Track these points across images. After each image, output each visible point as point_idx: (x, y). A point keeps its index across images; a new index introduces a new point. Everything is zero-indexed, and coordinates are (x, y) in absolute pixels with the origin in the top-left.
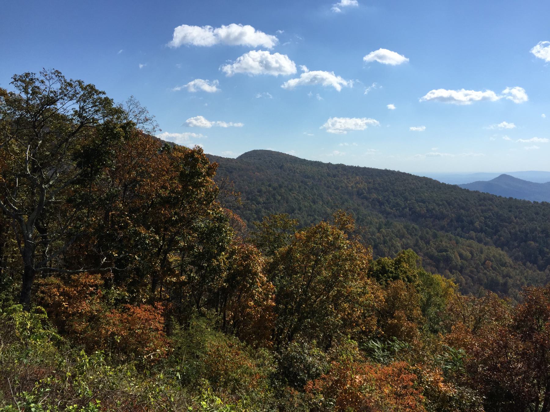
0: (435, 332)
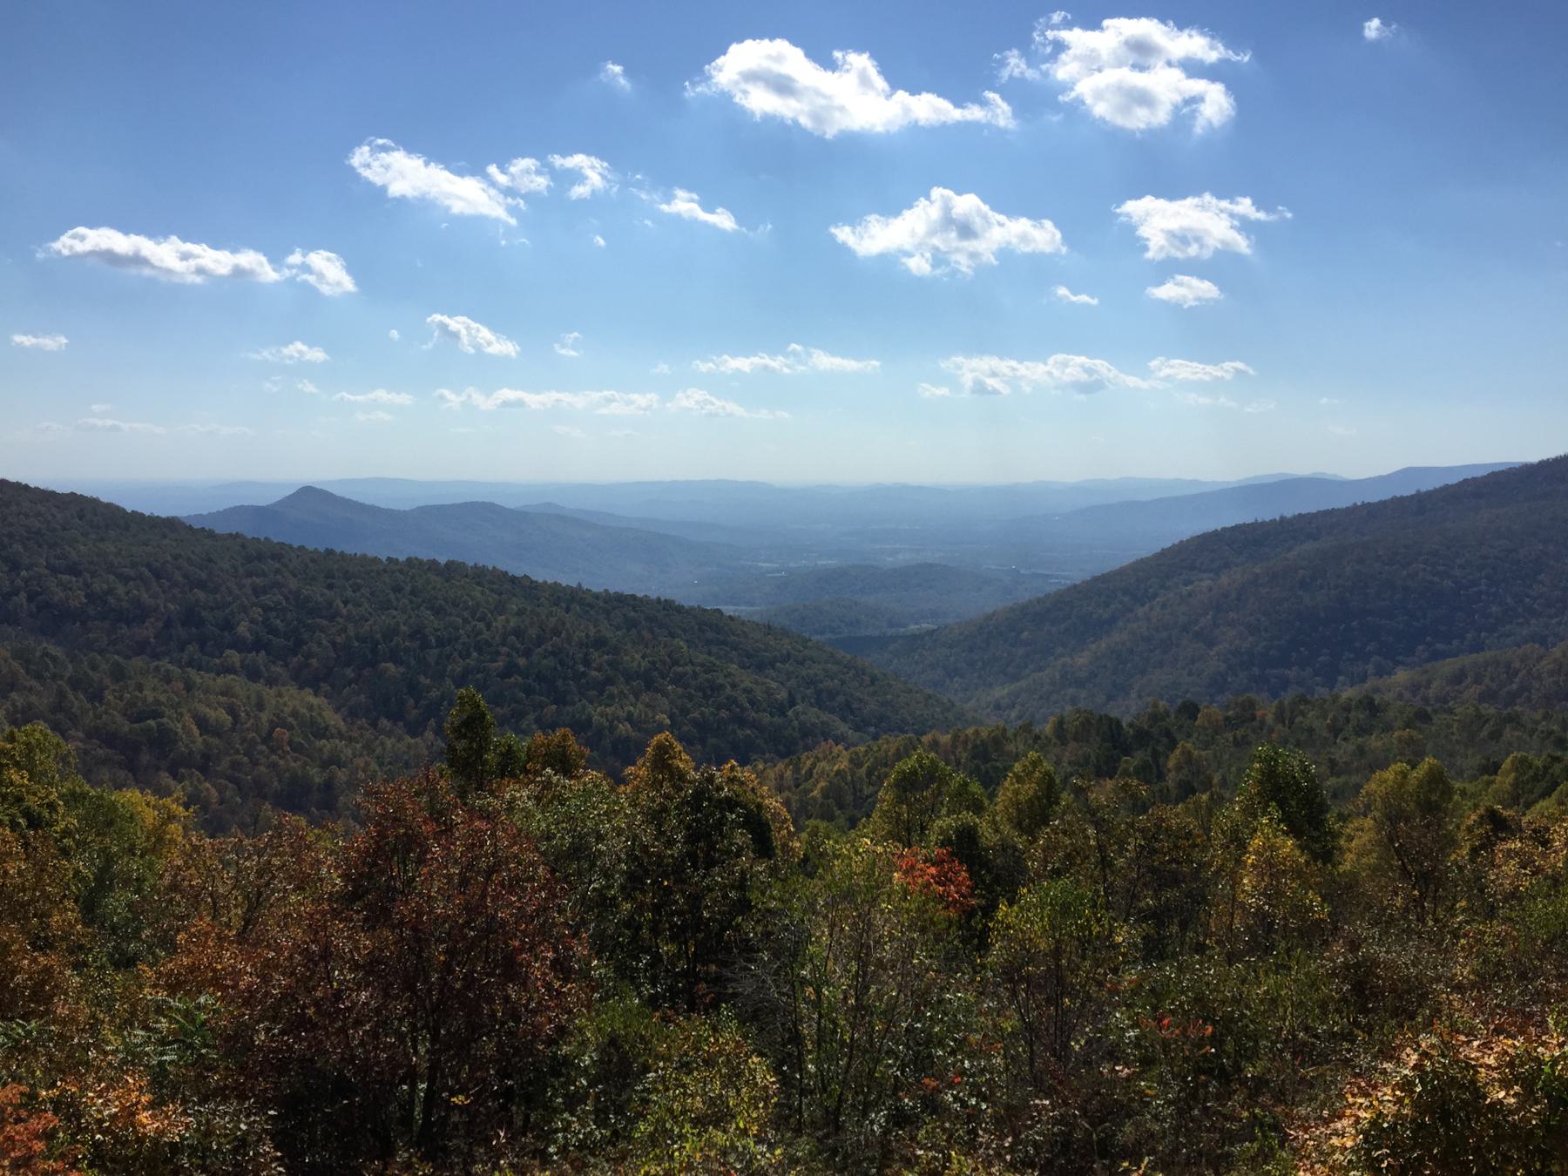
0: (125, 962)
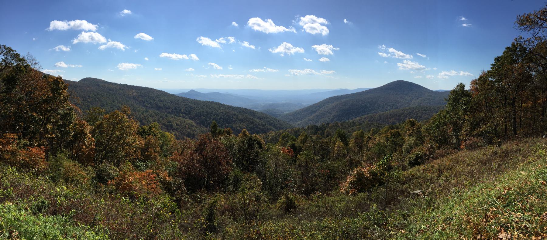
0: (166, 156)
